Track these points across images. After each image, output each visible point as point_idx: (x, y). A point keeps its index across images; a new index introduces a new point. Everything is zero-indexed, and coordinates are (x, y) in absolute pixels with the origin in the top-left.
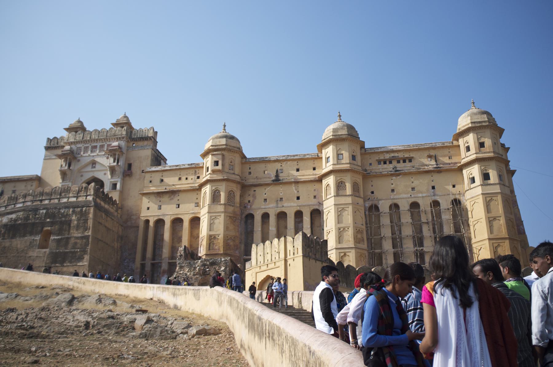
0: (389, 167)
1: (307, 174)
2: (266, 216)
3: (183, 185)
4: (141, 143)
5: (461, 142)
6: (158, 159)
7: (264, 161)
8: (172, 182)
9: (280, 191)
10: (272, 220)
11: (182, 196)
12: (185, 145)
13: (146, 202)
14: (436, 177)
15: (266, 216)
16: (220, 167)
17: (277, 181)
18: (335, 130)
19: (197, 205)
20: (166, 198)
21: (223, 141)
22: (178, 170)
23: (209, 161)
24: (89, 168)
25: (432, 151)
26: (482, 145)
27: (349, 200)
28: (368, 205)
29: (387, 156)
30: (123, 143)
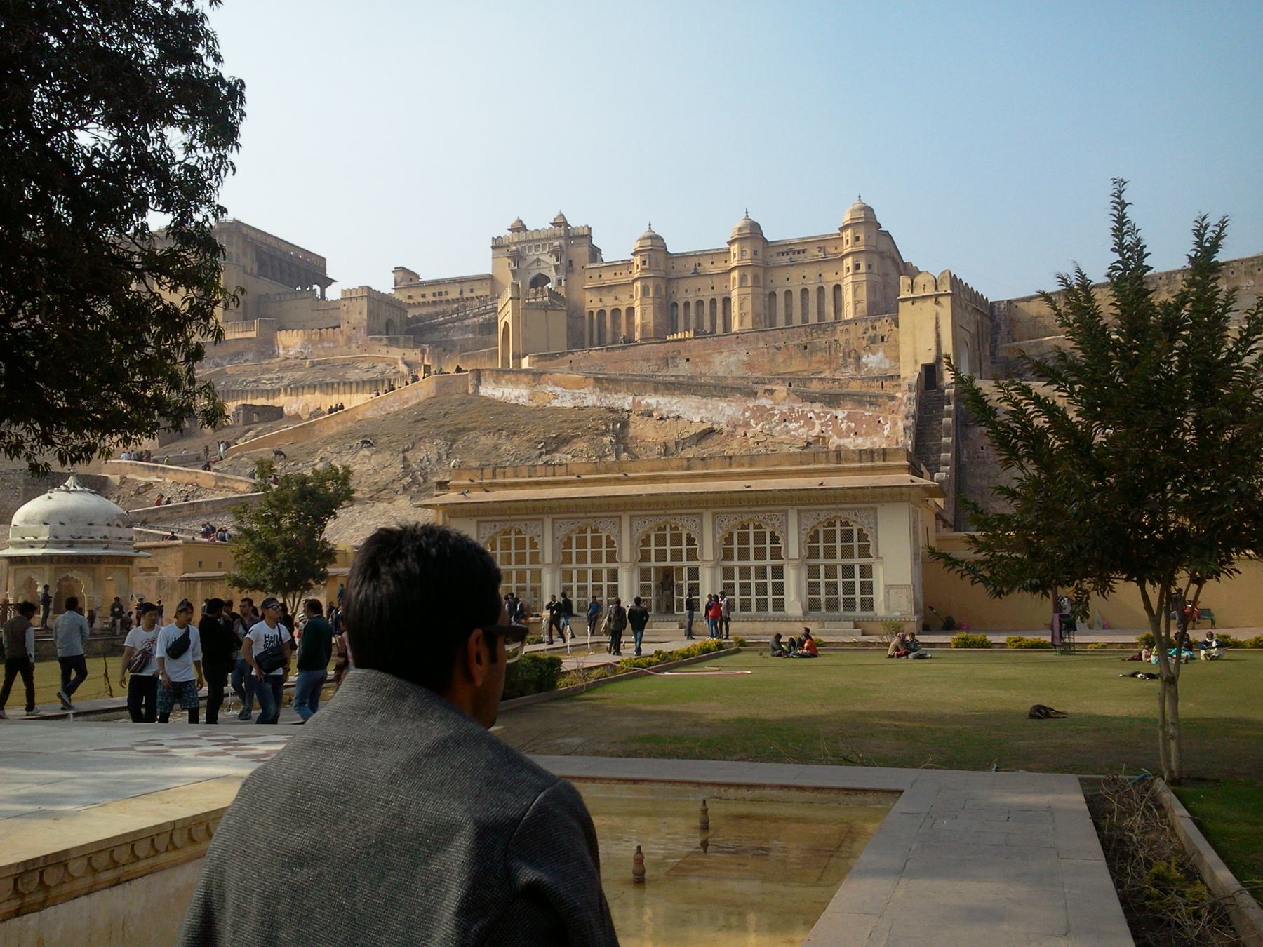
0: (786, 258)
1: (719, 267)
2: (687, 304)
3: (618, 280)
4: (577, 241)
5: (844, 235)
6: (595, 253)
7: (683, 256)
8: (608, 278)
9: (699, 282)
10: (692, 307)
11: (618, 289)
12: (617, 245)
13: (588, 296)
14: (824, 266)
15: (687, 304)
16: (647, 266)
17: (696, 274)
18: (740, 229)
19: (632, 296)
20: (605, 292)
21: (649, 242)
22: (612, 266)
23: (638, 260)
24: (535, 266)
25: (821, 242)
26: (857, 239)
27: (749, 290)
28: (767, 292)
29: (785, 249)
30: (562, 242)
